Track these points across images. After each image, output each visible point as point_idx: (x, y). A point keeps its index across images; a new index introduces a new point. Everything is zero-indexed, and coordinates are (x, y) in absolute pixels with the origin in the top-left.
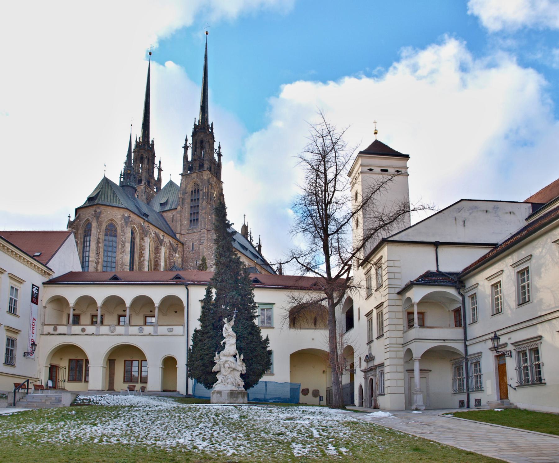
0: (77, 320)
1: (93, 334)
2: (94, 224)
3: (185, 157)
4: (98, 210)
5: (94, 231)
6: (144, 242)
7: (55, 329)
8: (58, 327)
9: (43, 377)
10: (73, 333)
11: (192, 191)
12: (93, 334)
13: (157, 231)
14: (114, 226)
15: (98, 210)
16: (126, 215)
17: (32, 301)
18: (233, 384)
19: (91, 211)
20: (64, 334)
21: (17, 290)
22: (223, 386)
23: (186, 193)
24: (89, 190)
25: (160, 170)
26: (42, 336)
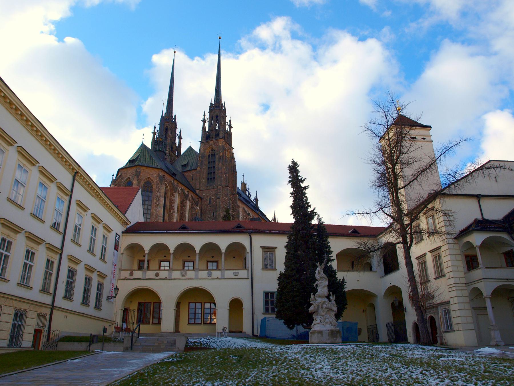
1: (166, 279)
3: (204, 128)
4: (139, 171)
6: (174, 197)
7: (131, 274)
10: (147, 277)
11: (209, 155)
12: (166, 279)
13: (183, 187)
14: (151, 184)
15: (139, 171)
16: (161, 175)
18: (331, 323)
19: (133, 170)
22: (322, 326)
23: (205, 157)
25: (180, 138)
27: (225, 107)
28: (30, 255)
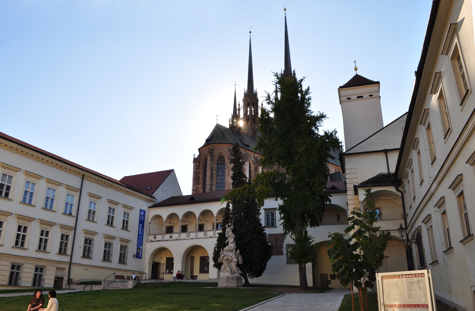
0: (170, 230)
2: (209, 158)
5: (209, 163)
7: (155, 238)
20: (160, 241)
24: (207, 133)
26: (148, 243)
27: (294, 74)
28: (44, 233)
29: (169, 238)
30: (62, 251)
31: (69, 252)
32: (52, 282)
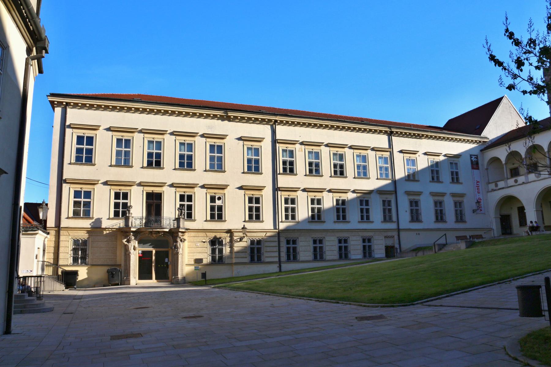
0: (515, 173)
1: (524, 183)
7: (496, 185)
8: (499, 183)
9: (495, 225)
10: (509, 185)
12: (524, 183)
17: (473, 168)
20: (503, 188)
21: (456, 164)
26: (489, 194)
29: (513, 184)
30: (387, 218)
31: (394, 218)
32: (383, 252)
